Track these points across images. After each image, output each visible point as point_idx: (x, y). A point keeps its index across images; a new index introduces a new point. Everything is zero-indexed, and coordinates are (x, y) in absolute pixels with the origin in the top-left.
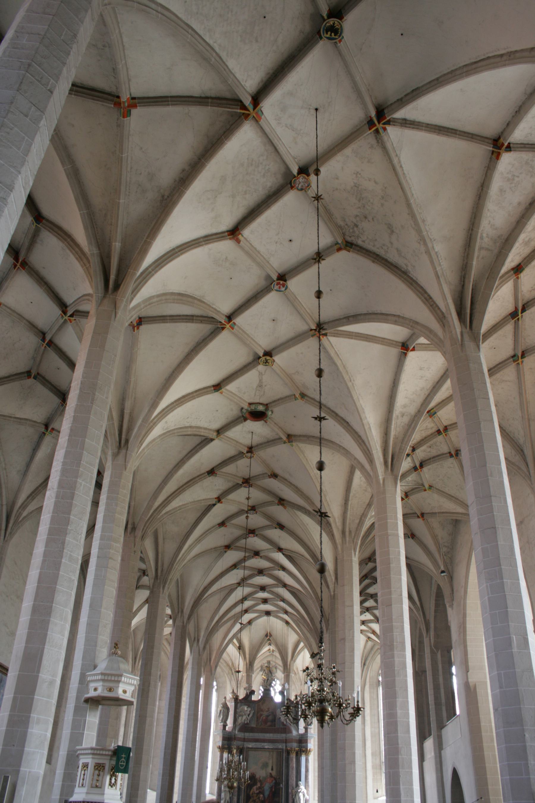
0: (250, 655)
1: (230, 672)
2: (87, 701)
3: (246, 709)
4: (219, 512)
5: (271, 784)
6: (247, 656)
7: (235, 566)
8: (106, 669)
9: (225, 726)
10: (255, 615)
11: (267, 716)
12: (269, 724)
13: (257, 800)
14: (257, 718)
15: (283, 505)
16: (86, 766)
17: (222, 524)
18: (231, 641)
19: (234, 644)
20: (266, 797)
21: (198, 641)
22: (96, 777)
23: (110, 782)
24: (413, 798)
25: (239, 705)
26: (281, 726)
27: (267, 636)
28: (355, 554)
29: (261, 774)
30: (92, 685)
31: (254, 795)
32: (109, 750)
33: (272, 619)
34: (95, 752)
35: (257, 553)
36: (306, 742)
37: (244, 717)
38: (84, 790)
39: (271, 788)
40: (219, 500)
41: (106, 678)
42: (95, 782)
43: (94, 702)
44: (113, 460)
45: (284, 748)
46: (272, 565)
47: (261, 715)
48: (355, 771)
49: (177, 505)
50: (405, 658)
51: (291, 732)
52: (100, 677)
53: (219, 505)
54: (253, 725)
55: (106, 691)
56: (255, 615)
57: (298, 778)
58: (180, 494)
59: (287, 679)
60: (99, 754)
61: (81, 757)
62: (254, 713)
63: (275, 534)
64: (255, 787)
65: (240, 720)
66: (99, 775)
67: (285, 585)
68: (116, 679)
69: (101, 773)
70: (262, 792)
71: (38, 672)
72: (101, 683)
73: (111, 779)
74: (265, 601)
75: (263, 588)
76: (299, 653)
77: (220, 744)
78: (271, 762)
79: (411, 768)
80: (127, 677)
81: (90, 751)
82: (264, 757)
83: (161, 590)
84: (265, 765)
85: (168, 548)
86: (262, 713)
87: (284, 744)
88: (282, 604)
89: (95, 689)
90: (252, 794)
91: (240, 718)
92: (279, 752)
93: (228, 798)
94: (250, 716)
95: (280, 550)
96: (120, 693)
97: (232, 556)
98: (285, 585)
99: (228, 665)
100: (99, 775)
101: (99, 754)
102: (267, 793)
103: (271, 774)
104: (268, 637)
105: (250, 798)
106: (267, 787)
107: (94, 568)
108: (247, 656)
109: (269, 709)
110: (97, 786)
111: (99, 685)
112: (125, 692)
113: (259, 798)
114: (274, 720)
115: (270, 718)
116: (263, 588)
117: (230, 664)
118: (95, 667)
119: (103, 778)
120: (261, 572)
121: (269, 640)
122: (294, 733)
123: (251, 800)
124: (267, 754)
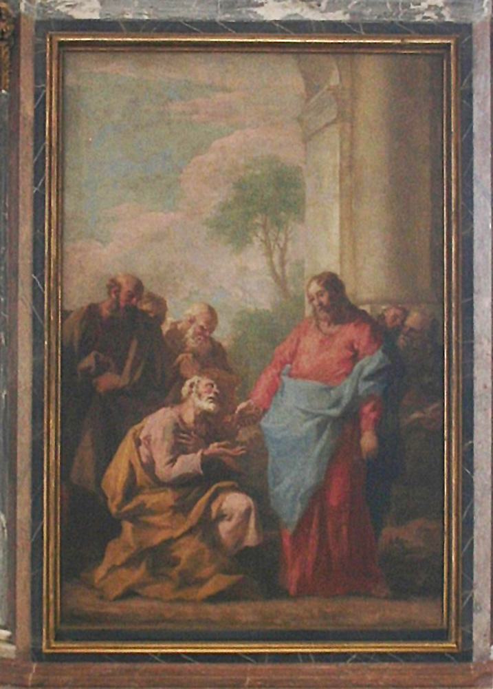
5: (346, 389)
13: (185, 551)
20: (290, 510)
29: (219, 285)
31: (151, 499)
39: (348, 421)
70: (248, 473)
78: (328, 157)
84: (268, 201)
90: (132, 489)
102: (294, 479)
103: (332, 283)
105: (112, 528)
106: (291, 421)
113: (207, 525)
123: (116, 553)
124: (286, 78)
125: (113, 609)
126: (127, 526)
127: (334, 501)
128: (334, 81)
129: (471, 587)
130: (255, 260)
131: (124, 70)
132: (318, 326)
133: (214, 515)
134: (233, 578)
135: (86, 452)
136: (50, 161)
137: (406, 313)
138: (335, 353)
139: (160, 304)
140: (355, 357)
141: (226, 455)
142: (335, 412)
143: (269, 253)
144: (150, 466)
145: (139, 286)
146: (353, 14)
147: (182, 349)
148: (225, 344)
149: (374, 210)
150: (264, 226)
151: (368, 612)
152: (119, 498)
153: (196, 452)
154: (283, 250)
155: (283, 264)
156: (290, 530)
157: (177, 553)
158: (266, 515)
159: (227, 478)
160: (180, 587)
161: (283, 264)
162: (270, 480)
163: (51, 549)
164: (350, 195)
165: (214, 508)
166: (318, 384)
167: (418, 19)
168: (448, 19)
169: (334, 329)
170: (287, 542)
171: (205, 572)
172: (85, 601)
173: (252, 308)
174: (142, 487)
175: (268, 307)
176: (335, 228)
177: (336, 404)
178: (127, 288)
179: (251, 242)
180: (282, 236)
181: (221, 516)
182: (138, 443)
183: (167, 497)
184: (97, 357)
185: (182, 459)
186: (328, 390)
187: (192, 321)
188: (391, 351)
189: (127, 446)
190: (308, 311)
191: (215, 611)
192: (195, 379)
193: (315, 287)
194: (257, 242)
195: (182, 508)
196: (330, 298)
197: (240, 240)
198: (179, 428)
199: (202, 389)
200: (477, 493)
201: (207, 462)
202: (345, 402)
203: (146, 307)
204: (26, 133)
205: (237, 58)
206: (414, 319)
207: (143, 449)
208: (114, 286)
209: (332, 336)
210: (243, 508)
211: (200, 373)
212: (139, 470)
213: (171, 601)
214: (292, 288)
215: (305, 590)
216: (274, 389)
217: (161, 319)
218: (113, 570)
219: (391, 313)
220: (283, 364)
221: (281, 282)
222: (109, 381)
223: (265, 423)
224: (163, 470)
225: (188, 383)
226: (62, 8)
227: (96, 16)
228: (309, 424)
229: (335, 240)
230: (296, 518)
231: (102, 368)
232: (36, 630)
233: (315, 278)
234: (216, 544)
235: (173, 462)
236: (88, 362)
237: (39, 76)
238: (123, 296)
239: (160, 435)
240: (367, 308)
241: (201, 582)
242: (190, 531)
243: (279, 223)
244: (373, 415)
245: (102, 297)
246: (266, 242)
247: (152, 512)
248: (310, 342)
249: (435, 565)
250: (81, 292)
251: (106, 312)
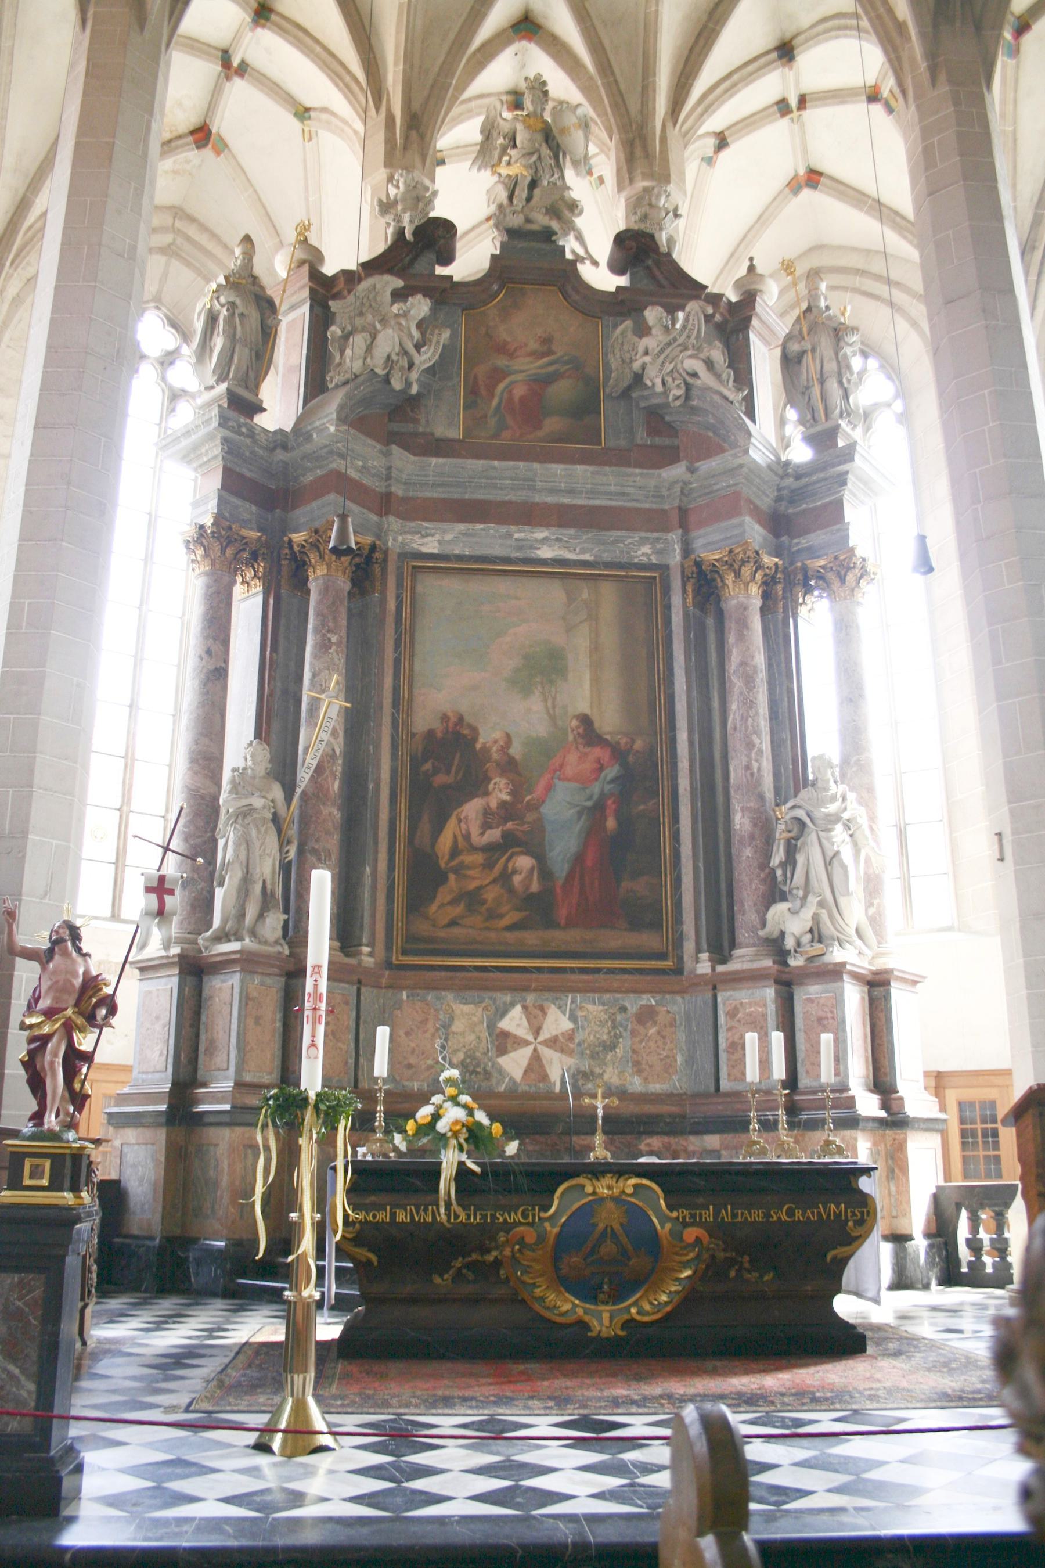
5: (596, 789)
13: (491, 895)
20: (560, 868)
29: (514, 721)
31: (468, 859)
36: (833, 514)
39: (597, 810)
45: (675, 558)
47: (498, 375)
64: (472, 809)
78: (582, 641)
84: (543, 668)
86: (501, 362)
87: (674, 537)
90: (455, 852)
103: (586, 721)
105: (441, 878)
113: (505, 877)
115: (563, 390)
123: (444, 895)
124: (555, 593)
125: (442, 934)
126: (452, 877)
127: (589, 863)
128: (585, 595)
129: (681, 923)
130: (536, 704)
131: (454, 584)
132: (577, 748)
133: (510, 871)
134: (523, 914)
135: (425, 827)
136: (406, 638)
137: (633, 741)
138: (588, 766)
139: (474, 730)
140: (601, 768)
141: (519, 833)
142: (589, 804)
143: (545, 700)
144: (467, 837)
145: (461, 719)
146: (596, 556)
147: (489, 760)
148: (517, 757)
149: (611, 676)
150: (542, 683)
152: (447, 857)
153: (497, 827)
154: (554, 699)
155: (554, 707)
156: (560, 882)
157: (485, 896)
158: (545, 872)
159: (519, 846)
160: (487, 920)
161: (554, 707)
162: (547, 848)
163: (400, 891)
164: (596, 667)
165: (510, 866)
166: (578, 785)
167: (636, 560)
168: (654, 561)
169: (587, 750)
170: (558, 890)
171: (505, 908)
172: (423, 928)
173: (534, 735)
174: (462, 851)
175: (545, 734)
176: (587, 685)
177: (590, 798)
178: (453, 719)
179: (533, 692)
180: (553, 689)
181: (515, 872)
182: (460, 821)
183: (479, 858)
184: (433, 764)
185: (489, 832)
186: (584, 789)
187: (496, 742)
188: (624, 765)
189: (451, 825)
190: (571, 738)
191: (510, 937)
192: (497, 779)
193: (574, 723)
194: (537, 693)
195: (489, 865)
196: (585, 730)
197: (526, 691)
198: (487, 812)
199: (502, 786)
200: (683, 860)
201: (505, 835)
202: (596, 797)
203: (466, 732)
204: (390, 621)
205: (525, 580)
206: (638, 745)
207: (463, 825)
208: (445, 718)
209: (586, 754)
210: (529, 866)
211: (501, 776)
212: (460, 839)
213: (481, 929)
214: (560, 723)
215: (570, 924)
216: (549, 788)
217: (475, 740)
218: (442, 907)
219: (624, 740)
220: (555, 771)
221: (553, 718)
222: (440, 779)
223: (545, 810)
224: (476, 840)
225: (493, 782)
226: (415, 546)
227: (436, 551)
228: (572, 811)
229: (587, 693)
230: (564, 874)
231: (436, 771)
232: (388, 948)
233: (575, 717)
234: (511, 890)
235: (482, 834)
236: (428, 766)
237: (399, 585)
238: (451, 724)
239: (474, 816)
240: (608, 737)
241: (501, 916)
242: (494, 881)
243: (551, 682)
244: (613, 806)
245: (437, 725)
246: (543, 693)
247: (469, 868)
248: (572, 758)
249: (657, 908)
250: (424, 720)
251: (439, 735)
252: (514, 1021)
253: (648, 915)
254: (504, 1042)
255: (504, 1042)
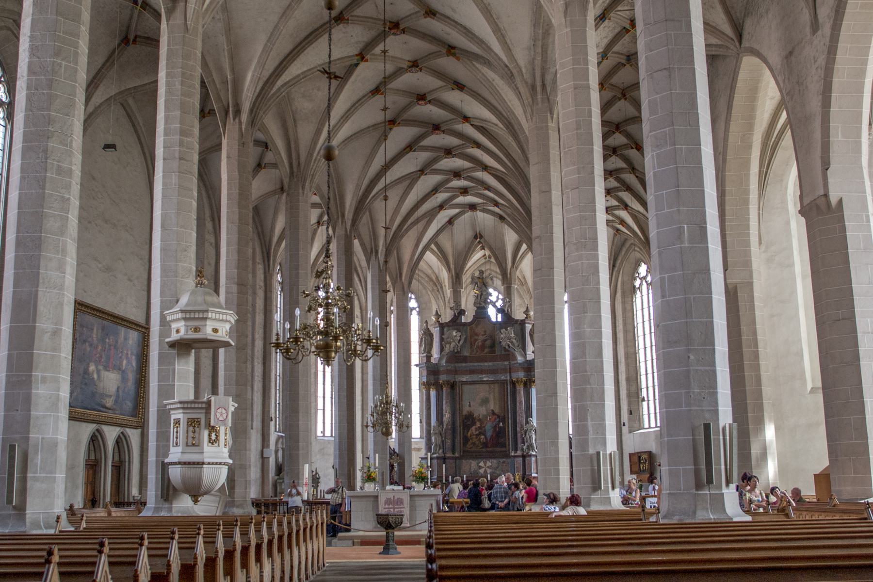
0: (455, 264)
1: (435, 288)
2: (173, 345)
3: (454, 333)
4: (367, 75)
6: (452, 266)
7: (410, 147)
8: (187, 305)
9: (429, 357)
10: (457, 211)
11: (485, 341)
12: (486, 350)
14: (471, 344)
15: (454, 55)
16: (177, 422)
17: (376, 91)
18: (426, 248)
19: (433, 251)
21: (377, 252)
22: (191, 435)
23: (210, 439)
24: (605, 435)
25: (445, 330)
26: (503, 352)
27: (476, 237)
28: (552, 118)
29: (480, 411)
30: (174, 326)
32: (202, 403)
33: (480, 215)
34: (186, 406)
35: (436, 127)
37: (453, 345)
38: (179, 449)
40: (362, 56)
41: (188, 316)
42: (190, 440)
43: (183, 346)
44: (168, 21)
46: (462, 142)
47: (476, 340)
48: (557, 405)
49: (300, 72)
50: (598, 260)
51: (515, 358)
52: (180, 315)
53: (363, 65)
54: (466, 353)
55: (190, 332)
56: (457, 211)
57: (529, 414)
58: (298, 54)
59: (508, 293)
60: (191, 408)
61: (172, 412)
62: (466, 339)
63: (454, 97)
64: (473, 428)
65: (447, 349)
66: (194, 432)
67: (486, 168)
68: (201, 316)
69: (197, 430)
71: (34, 321)
72: (182, 323)
73: (210, 435)
74: (465, 191)
75: (457, 174)
76: (522, 257)
77: (425, 380)
78: (492, 396)
79: (602, 399)
80: (216, 312)
81: (179, 406)
82: (482, 391)
83: (301, 191)
84: (485, 401)
85: (305, 133)
88: (487, 192)
89: (178, 331)
91: (448, 346)
92: (503, 383)
93: (439, 442)
94: (461, 342)
95: (466, 119)
96: (208, 331)
97: (401, 136)
98: (486, 168)
99: (431, 280)
100: (194, 432)
101: (191, 408)
104: (478, 238)
107: (161, 174)
108: (452, 266)
109: (485, 332)
110: (193, 445)
111: (181, 325)
112: (215, 331)
113: (480, 439)
114: (493, 346)
115: (488, 343)
116: (457, 174)
117: (434, 278)
118: (177, 301)
119: (199, 434)
120: (448, 152)
121: (479, 242)
122: (520, 359)
124: (486, 387)
131: (468, 386)
151: (498, 449)
158: (486, 437)
164: (494, 399)
250: (465, 413)
252: (482, 464)
253: (504, 445)
254: (480, 467)
255: (480, 467)
